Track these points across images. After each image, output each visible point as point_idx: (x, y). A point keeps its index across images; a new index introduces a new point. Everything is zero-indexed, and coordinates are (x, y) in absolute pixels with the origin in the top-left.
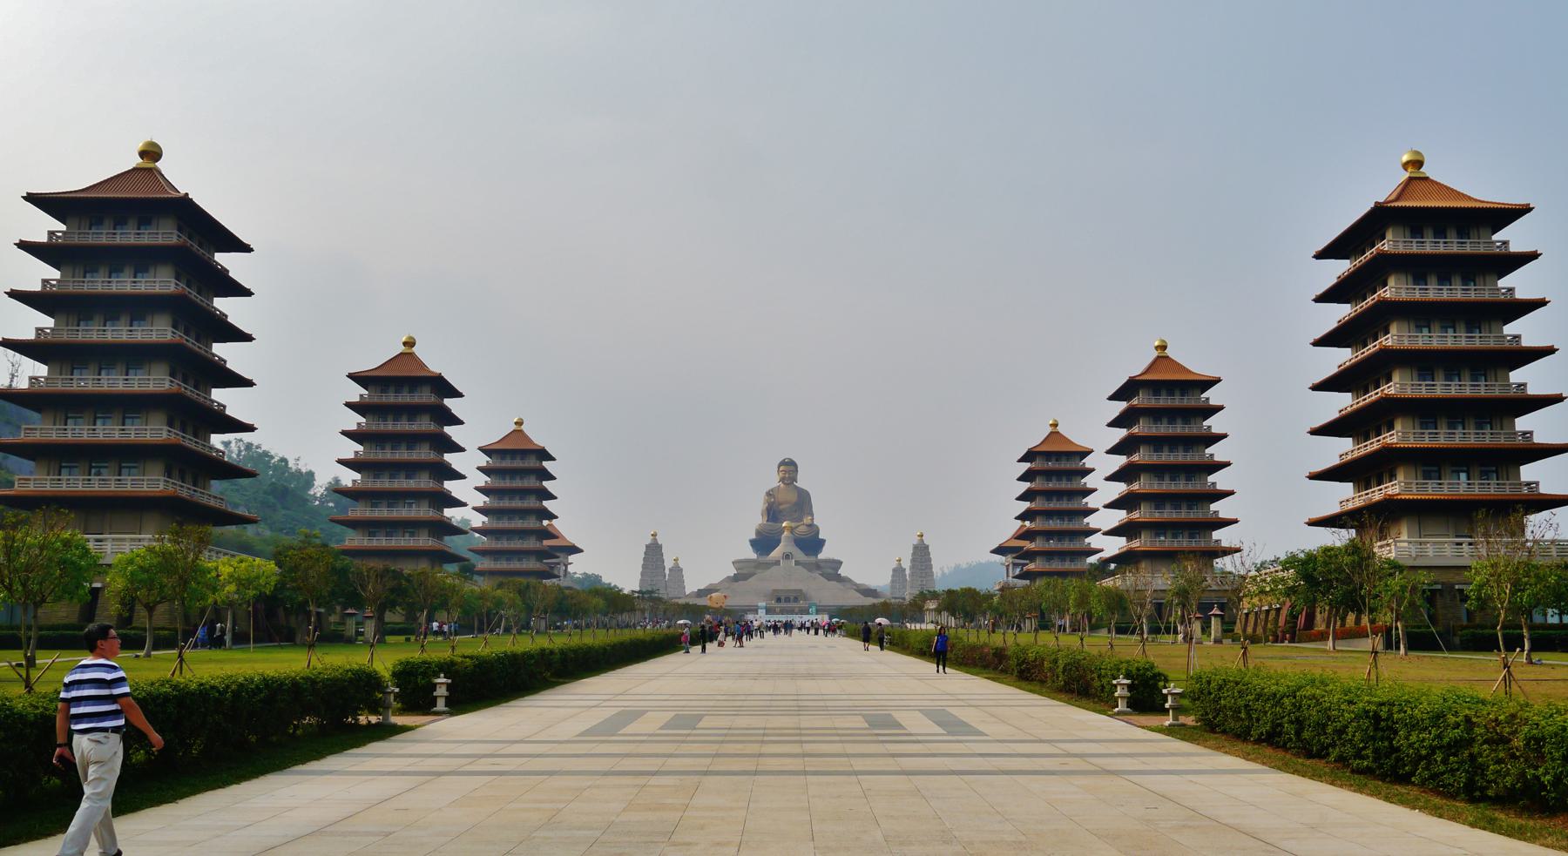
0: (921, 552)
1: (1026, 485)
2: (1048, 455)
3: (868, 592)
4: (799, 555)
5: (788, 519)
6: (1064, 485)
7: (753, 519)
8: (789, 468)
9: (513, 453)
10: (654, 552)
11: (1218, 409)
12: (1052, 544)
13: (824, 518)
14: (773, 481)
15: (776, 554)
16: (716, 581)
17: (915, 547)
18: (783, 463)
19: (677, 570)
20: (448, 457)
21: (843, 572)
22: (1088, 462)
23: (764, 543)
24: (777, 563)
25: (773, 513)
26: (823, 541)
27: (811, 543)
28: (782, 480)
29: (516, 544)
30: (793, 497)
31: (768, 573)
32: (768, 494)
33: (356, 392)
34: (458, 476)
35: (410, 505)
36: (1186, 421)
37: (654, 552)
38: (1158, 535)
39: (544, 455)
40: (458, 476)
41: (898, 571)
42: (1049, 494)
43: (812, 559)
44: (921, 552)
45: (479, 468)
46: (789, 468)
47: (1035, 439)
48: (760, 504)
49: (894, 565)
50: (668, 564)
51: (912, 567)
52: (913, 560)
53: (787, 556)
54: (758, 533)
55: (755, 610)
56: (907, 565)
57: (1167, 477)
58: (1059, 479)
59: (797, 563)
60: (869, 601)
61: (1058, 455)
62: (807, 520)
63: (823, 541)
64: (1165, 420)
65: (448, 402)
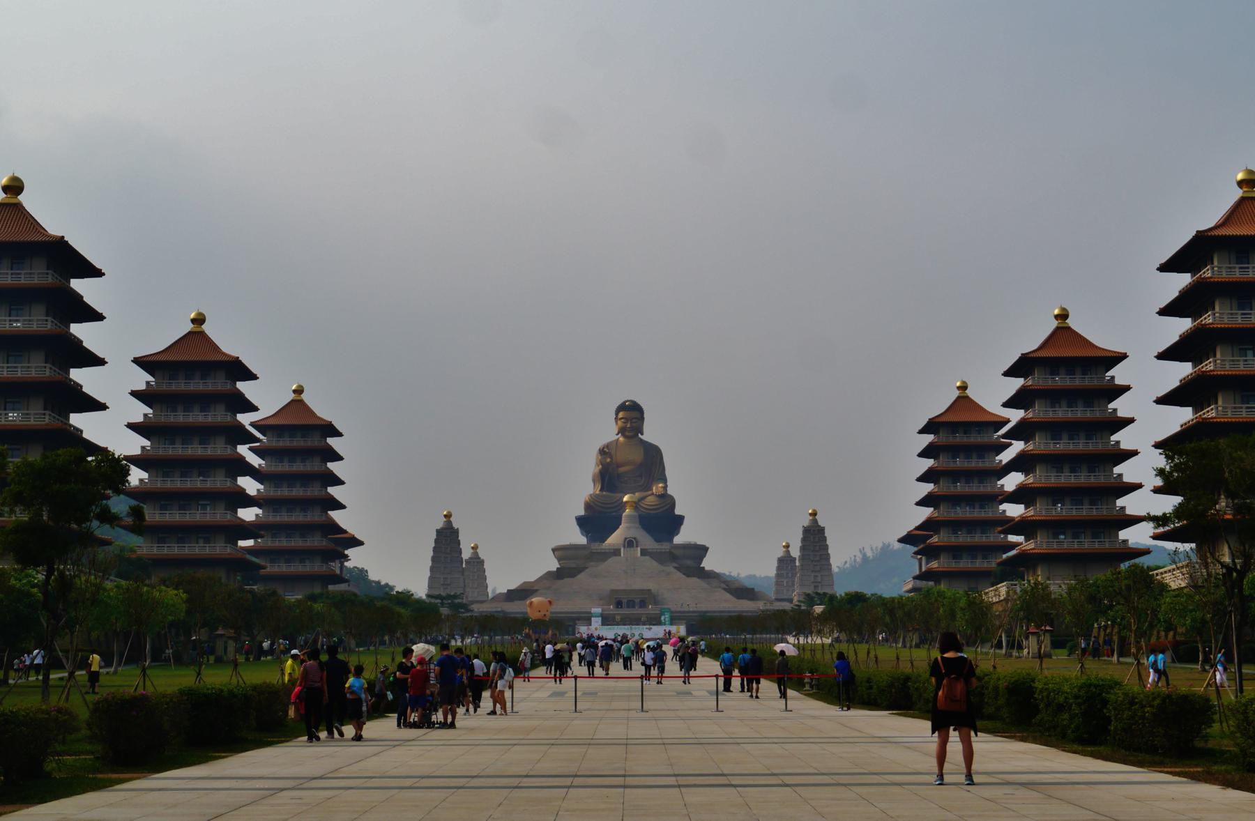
0: (814, 536)
1: (929, 463)
2: (953, 427)
3: (743, 591)
4: (647, 541)
6: (974, 463)
7: (581, 488)
8: (631, 415)
9: (291, 430)
10: (447, 538)
11: (1126, 389)
12: (963, 538)
13: (681, 484)
14: (609, 432)
15: (615, 539)
16: (532, 577)
17: (807, 531)
18: (622, 407)
19: (477, 562)
20: (76, 374)
21: (708, 564)
22: (1119, 374)
23: (597, 521)
24: (616, 552)
25: (609, 476)
26: (680, 519)
27: (664, 521)
28: (622, 431)
29: (297, 542)
30: (637, 456)
31: (603, 567)
32: (603, 452)
33: (142, 379)
34: (95, 406)
35: (204, 507)
36: (1089, 404)
37: (447, 538)
38: (1056, 535)
39: (240, 371)
40: (95, 406)
41: (785, 562)
42: (954, 475)
43: (665, 546)
44: (814, 536)
45: (135, 394)
46: (631, 415)
47: (939, 404)
48: (589, 466)
49: (780, 553)
50: (466, 554)
51: (802, 558)
52: (803, 549)
53: (630, 543)
54: (588, 506)
55: (587, 619)
56: (795, 552)
57: (1066, 468)
58: (968, 457)
59: (644, 552)
60: (746, 606)
61: (967, 427)
62: (657, 488)
63: (680, 519)
64: (1064, 403)
65: (77, 284)
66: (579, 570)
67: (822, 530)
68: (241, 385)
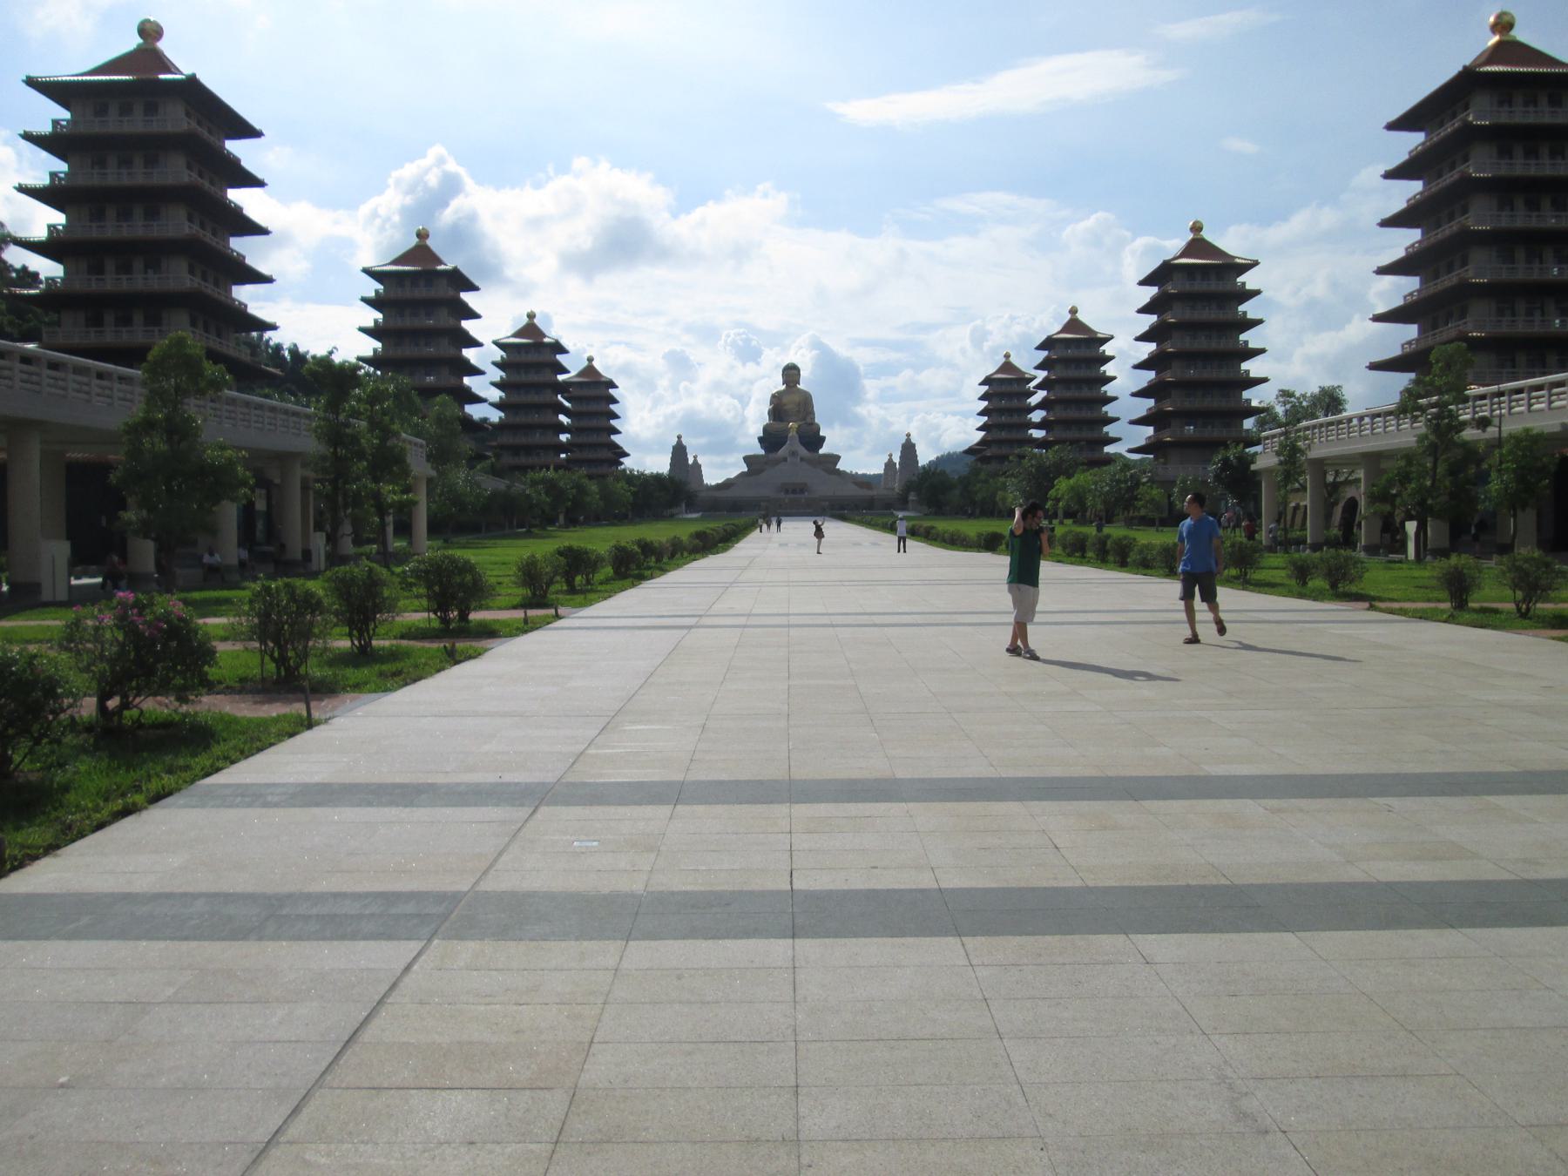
0: (909, 449)
4: (803, 451)
5: (792, 420)
10: (679, 451)
15: (782, 452)
19: (697, 466)
21: (840, 466)
22: (1108, 349)
23: (771, 439)
24: (785, 460)
26: (823, 439)
27: (813, 439)
39: (558, 348)
41: (890, 465)
49: (886, 459)
50: (691, 461)
56: (896, 460)
63: (823, 439)
66: (762, 471)
67: (913, 446)
68: (559, 357)
